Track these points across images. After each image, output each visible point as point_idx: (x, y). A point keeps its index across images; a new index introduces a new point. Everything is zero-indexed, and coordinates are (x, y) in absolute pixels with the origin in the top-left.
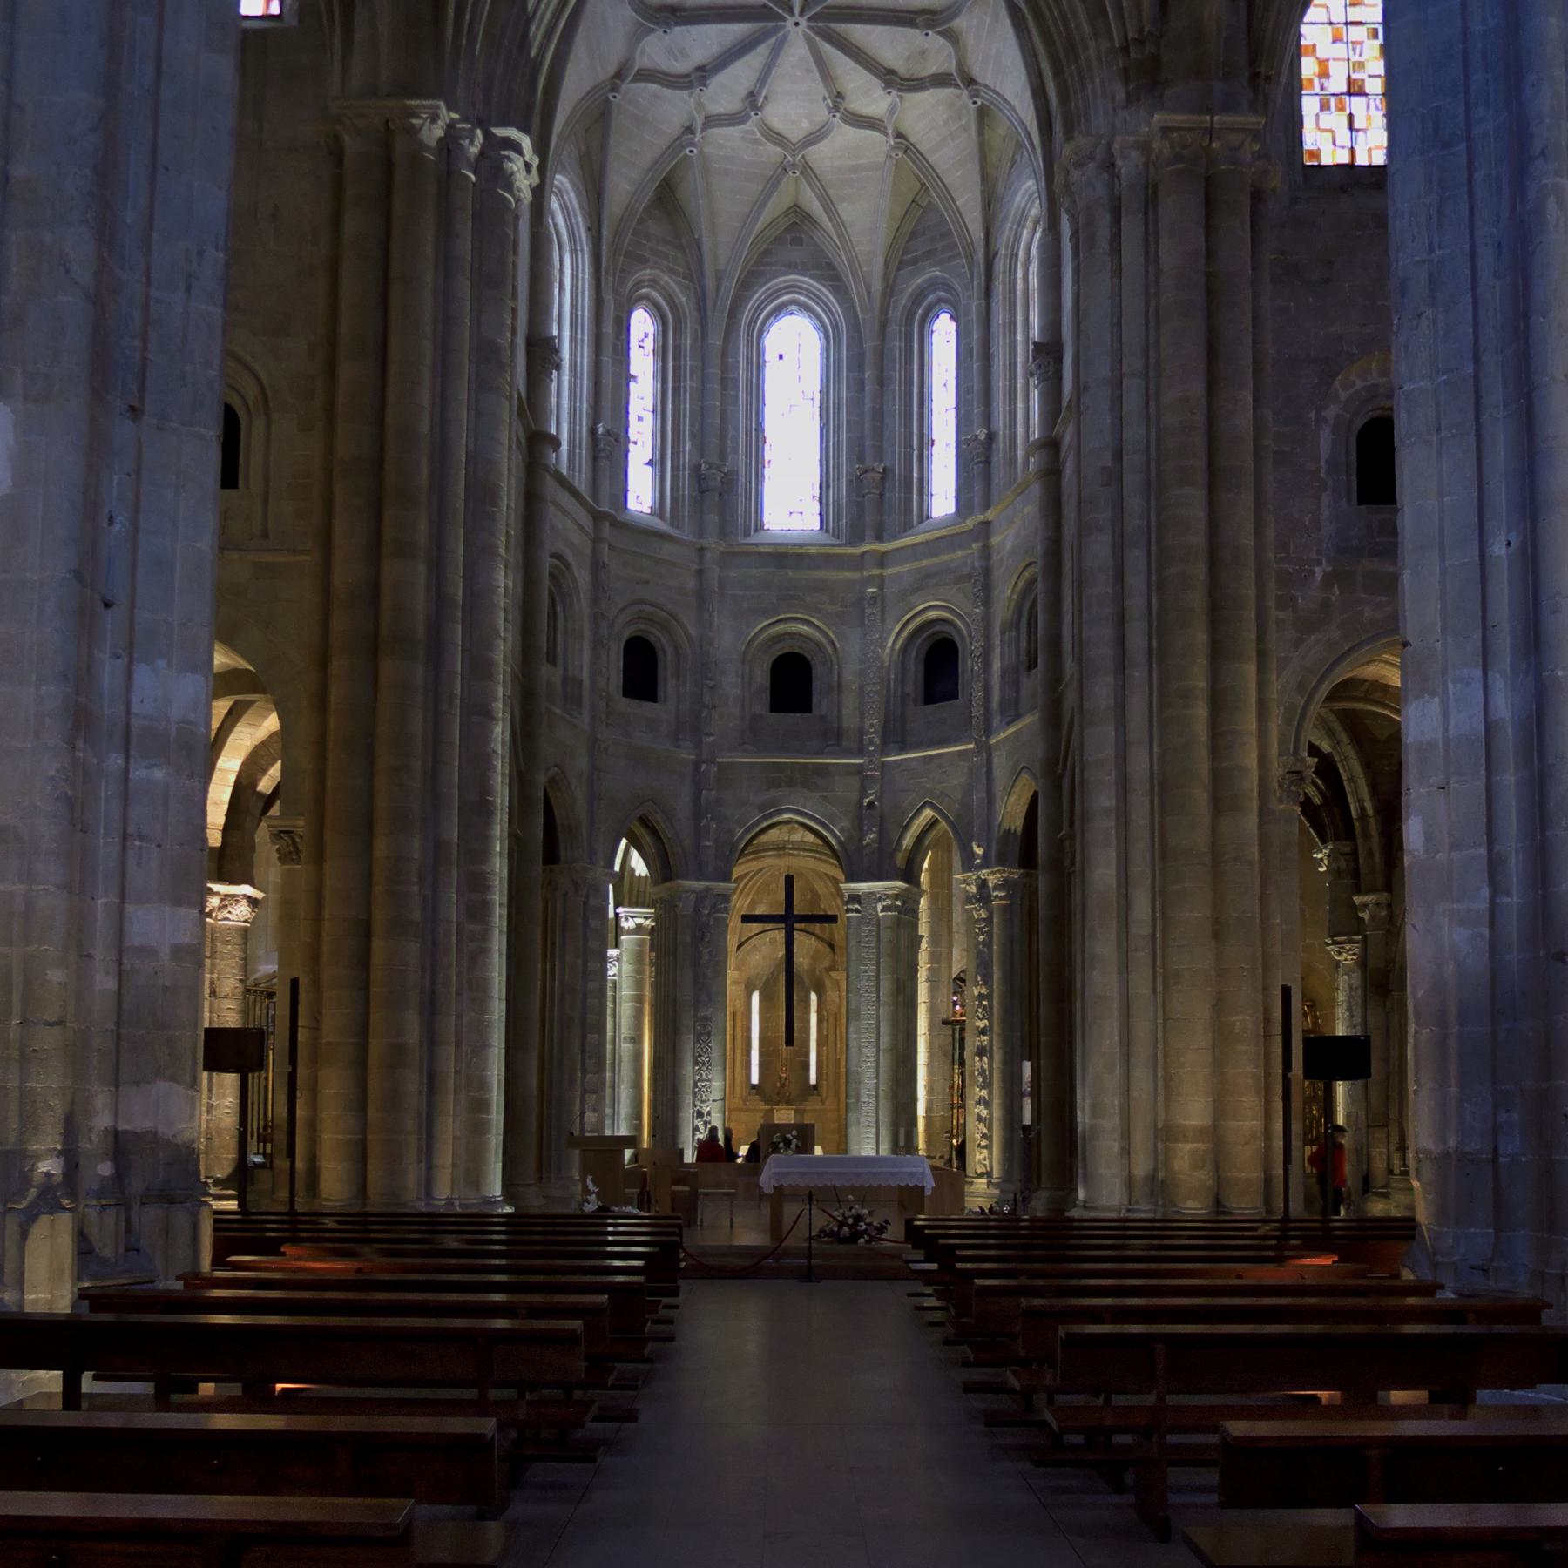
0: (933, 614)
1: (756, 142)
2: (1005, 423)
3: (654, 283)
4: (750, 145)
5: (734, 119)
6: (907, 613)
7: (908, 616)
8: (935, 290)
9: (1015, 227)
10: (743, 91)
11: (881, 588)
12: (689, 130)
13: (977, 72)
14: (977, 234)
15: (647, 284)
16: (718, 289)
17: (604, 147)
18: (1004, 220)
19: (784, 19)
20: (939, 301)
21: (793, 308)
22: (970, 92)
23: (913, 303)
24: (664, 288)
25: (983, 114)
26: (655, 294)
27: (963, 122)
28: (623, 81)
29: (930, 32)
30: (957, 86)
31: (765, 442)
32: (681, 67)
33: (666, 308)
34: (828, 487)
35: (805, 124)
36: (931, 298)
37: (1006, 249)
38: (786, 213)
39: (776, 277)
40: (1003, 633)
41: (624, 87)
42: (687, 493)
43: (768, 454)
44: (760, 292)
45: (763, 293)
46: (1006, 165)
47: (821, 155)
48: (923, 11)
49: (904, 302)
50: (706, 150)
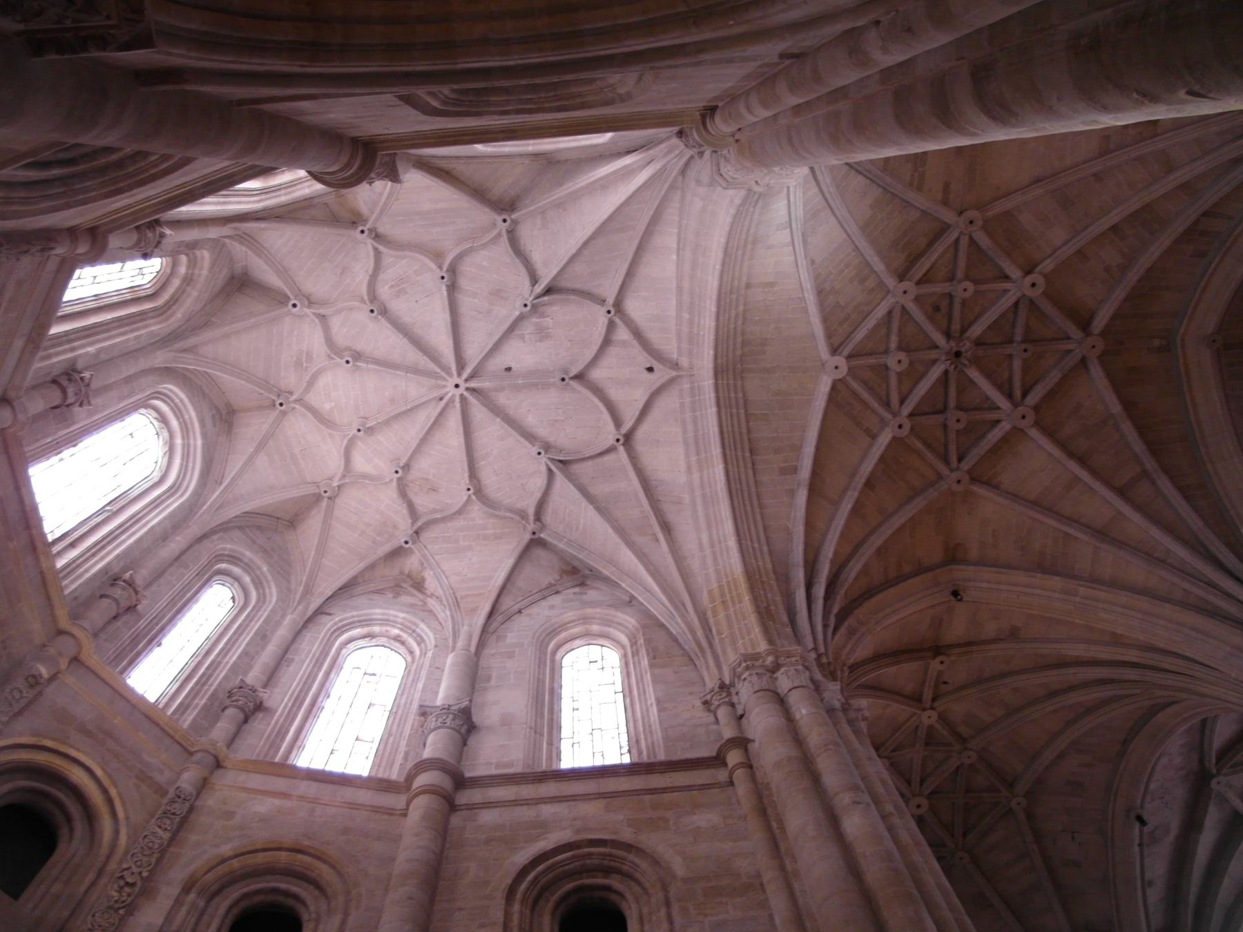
0: (78, 776)
1: (298, 364)
2: (283, 712)
3: (188, 280)
4: (294, 359)
5: (329, 341)
6: (53, 739)
7: (49, 743)
8: (247, 572)
9: (356, 619)
10: (359, 347)
11: (53, 678)
12: (310, 301)
13: (426, 536)
14: (326, 588)
15: (190, 272)
16: (185, 351)
17: (314, 221)
18: (355, 608)
19: (450, 375)
20: (237, 579)
21: (166, 434)
22: (412, 534)
23: (228, 556)
24: (183, 292)
25: (397, 553)
26: (176, 283)
27: (378, 538)
28: (373, 239)
29: (471, 492)
30: (413, 523)
31: (74, 446)
32: (384, 291)
33: (166, 296)
34: (73, 545)
35: (327, 406)
36: (237, 570)
37: (340, 621)
38: (228, 405)
39: (195, 409)
40: (186, 889)
41: (369, 241)
42: (55, 360)
43: (66, 453)
44: (183, 396)
45: (181, 400)
46: (372, 587)
47: (299, 427)
48: (479, 481)
49: (228, 546)
50: (288, 319)
